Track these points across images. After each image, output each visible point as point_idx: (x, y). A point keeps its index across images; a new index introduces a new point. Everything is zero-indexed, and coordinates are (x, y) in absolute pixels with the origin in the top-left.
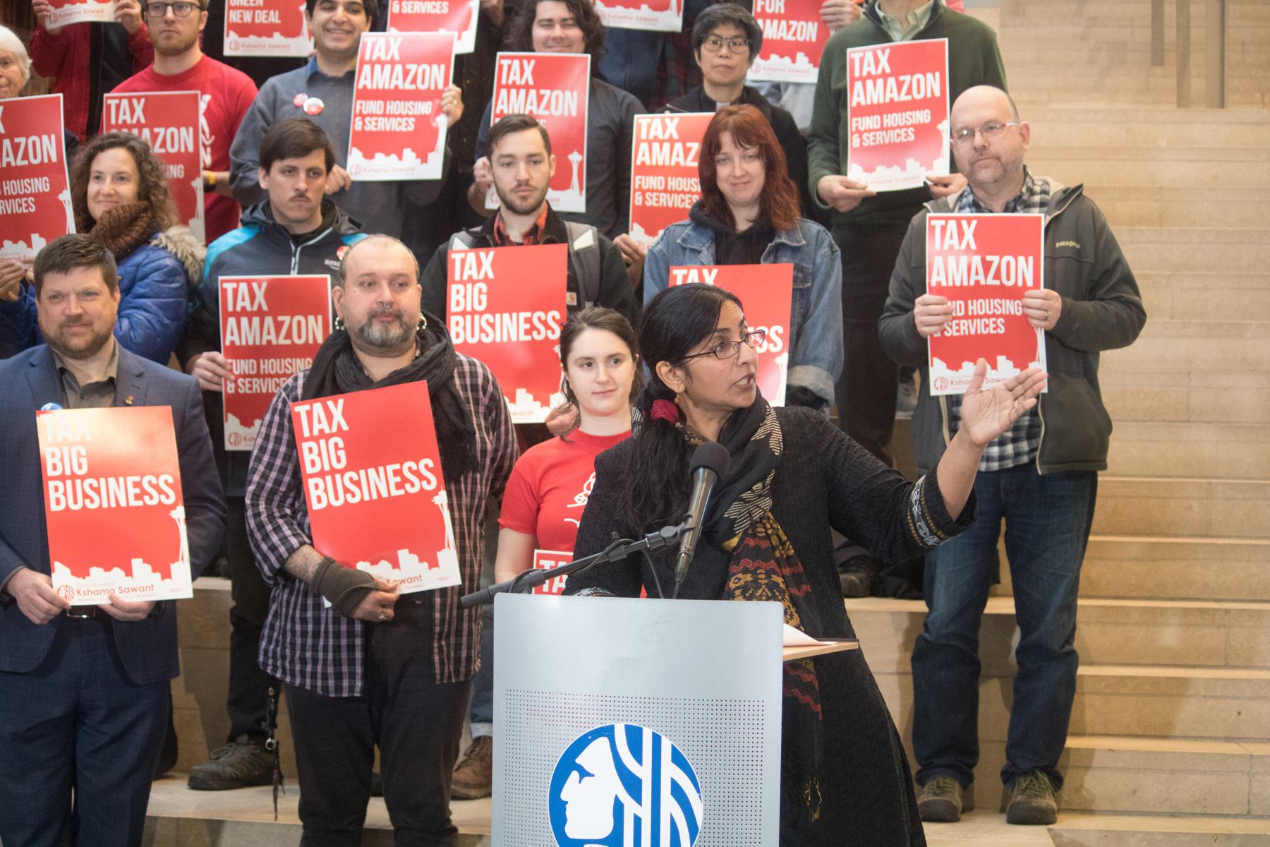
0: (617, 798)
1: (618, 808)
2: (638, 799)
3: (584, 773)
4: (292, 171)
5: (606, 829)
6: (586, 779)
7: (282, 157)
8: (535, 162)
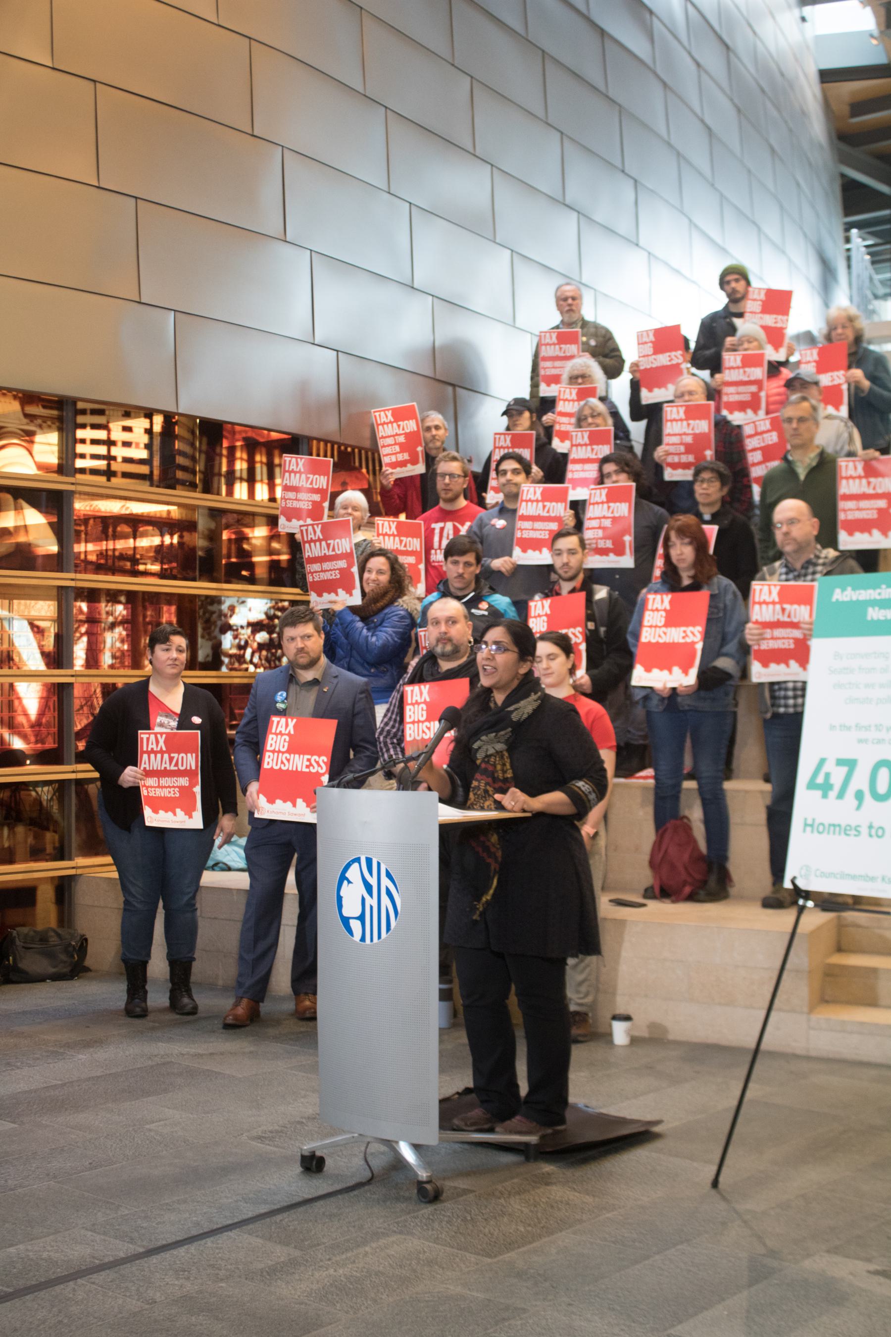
1: (363, 900)
3: (349, 882)
4: (456, 563)
5: (358, 913)
6: (350, 885)
7: (452, 555)
8: (573, 554)
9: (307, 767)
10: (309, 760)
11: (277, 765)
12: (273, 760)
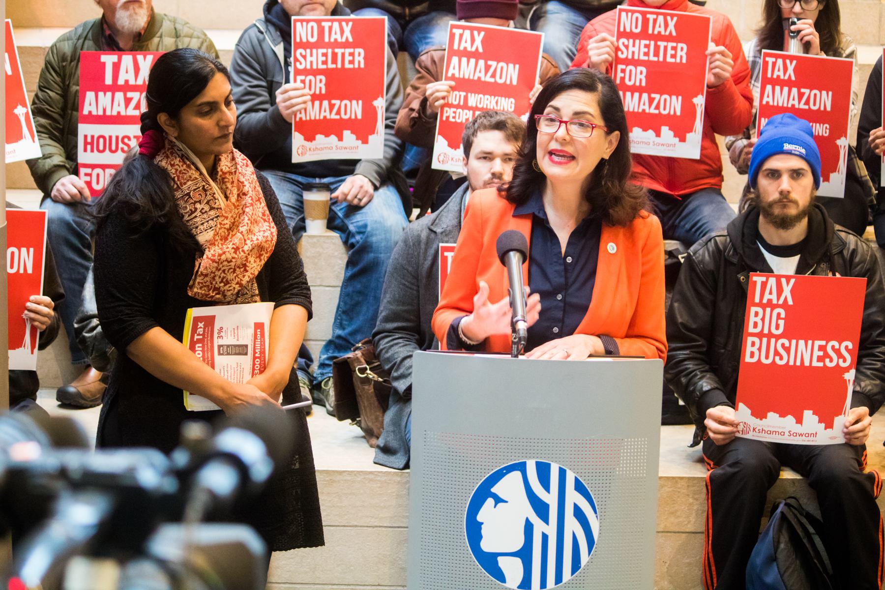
0: (527, 520)
2: (547, 523)
5: (518, 543)
9: (820, 359)
10: (822, 348)
11: (767, 357)
12: (760, 349)
